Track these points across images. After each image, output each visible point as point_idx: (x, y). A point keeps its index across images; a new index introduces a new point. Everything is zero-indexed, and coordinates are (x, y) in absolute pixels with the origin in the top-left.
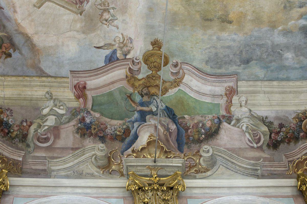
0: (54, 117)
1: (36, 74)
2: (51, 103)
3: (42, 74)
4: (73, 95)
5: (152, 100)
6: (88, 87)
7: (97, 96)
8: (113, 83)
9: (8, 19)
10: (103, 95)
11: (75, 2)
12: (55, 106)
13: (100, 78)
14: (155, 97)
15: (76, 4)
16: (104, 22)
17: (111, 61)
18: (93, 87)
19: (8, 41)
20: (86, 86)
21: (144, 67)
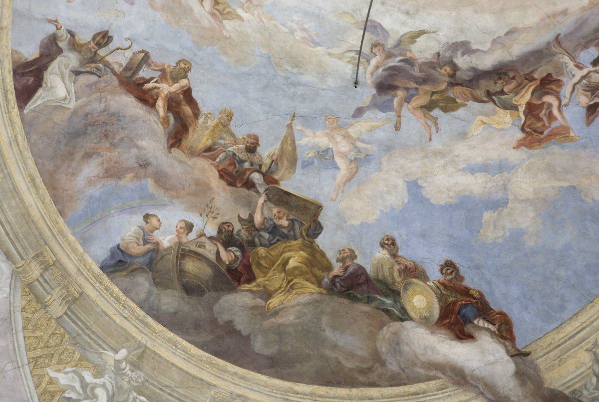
9: (581, 24)
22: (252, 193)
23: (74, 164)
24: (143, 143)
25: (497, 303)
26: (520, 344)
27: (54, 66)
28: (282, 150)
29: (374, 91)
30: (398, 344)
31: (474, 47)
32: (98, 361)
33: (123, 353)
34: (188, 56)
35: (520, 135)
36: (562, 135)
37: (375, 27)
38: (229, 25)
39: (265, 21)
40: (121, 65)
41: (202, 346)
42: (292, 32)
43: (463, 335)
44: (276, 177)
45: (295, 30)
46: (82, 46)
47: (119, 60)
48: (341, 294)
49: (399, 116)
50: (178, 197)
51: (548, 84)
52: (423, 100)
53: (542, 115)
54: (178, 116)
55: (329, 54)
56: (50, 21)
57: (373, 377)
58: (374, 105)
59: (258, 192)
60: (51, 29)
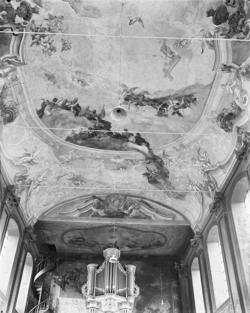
0: (236, 89)
1: (210, 89)
2: (228, 87)
3: (211, 86)
4: (227, 73)
5: (246, 25)
6: (225, 64)
7: (232, 60)
8: (227, 48)
9: (176, 94)
10: (233, 56)
11: (173, 60)
12: (230, 85)
13: (221, 55)
14: (246, 22)
15: (174, 59)
16: (187, 45)
17: (213, 46)
18: (226, 60)
19: (188, 97)
20: (224, 64)
21: (222, 25)
22: (95, 121)
23: (55, 125)
24: (70, 118)
25: (147, 140)
26: (150, 148)
27: (46, 109)
28: (102, 113)
29: (124, 100)
30: (127, 145)
31: (149, 93)
32: (68, 153)
33: (72, 151)
34: (76, 97)
35: (157, 113)
36: (166, 116)
37: (125, 86)
38: (86, 87)
39: (96, 85)
40: (61, 105)
41: (88, 147)
42: (103, 87)
43: (140, 145)
44: (101, 118)
45: (104, 87)
46: (51, 103)
47: (60, 103)
48: (115, 138)
49: (130, 106)
50: (79, 125)
51: (166, 105)
52: (136, 103)
53: (163, 111)
54: (77, 110)
55: (113, 92)
56: (42, 99)
57: (121, 150)
58: (124, 103)
59: (97, 121)
60: (43, 101)
